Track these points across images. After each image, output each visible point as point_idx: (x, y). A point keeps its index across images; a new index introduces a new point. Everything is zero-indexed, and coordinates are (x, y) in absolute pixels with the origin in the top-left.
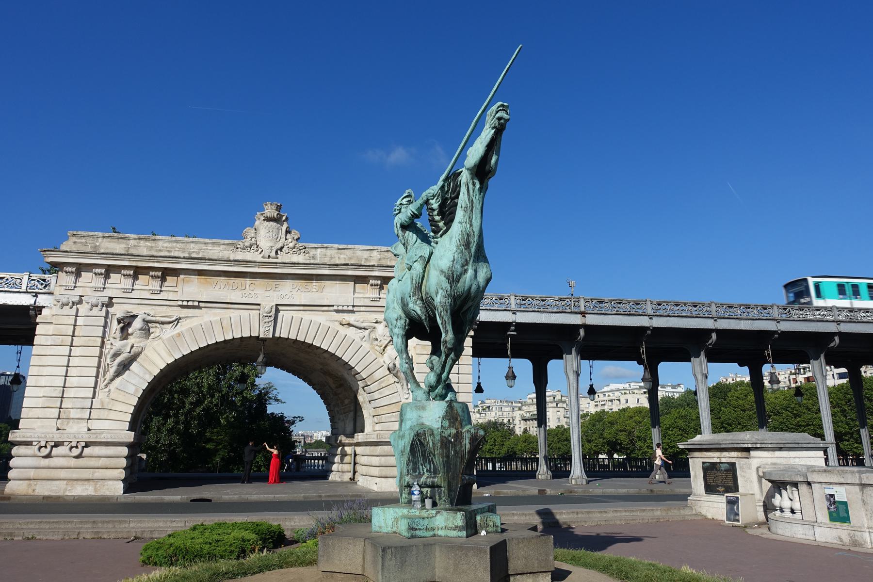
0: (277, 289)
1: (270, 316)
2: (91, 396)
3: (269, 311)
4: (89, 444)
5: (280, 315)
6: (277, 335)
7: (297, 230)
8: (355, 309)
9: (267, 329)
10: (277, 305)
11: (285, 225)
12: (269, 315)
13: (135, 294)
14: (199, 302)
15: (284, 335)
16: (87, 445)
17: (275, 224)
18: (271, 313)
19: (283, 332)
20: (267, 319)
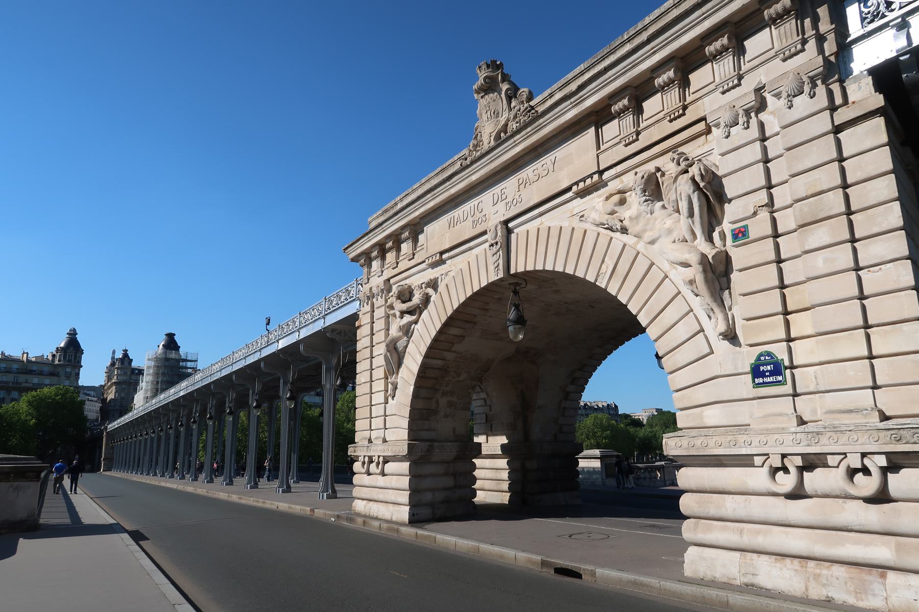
0: (504, 197)
1: (497, 243)
2: (383, 401)
3: (494, 235)
4: (388, 459)
5: (513, 236)
6: (512, 271)
7: (524, 88)
8: (606, 175)
9: (496, 265)
10: (506, 222)
11: (505, 87)
12: (493, 242)
13: (403, 265)
14: (442, 253)
15: (521, 269)
16: (386, 461)
17: (491, 95)
18: (497, 238)
19: (519, 265)
20: (495, 249)
